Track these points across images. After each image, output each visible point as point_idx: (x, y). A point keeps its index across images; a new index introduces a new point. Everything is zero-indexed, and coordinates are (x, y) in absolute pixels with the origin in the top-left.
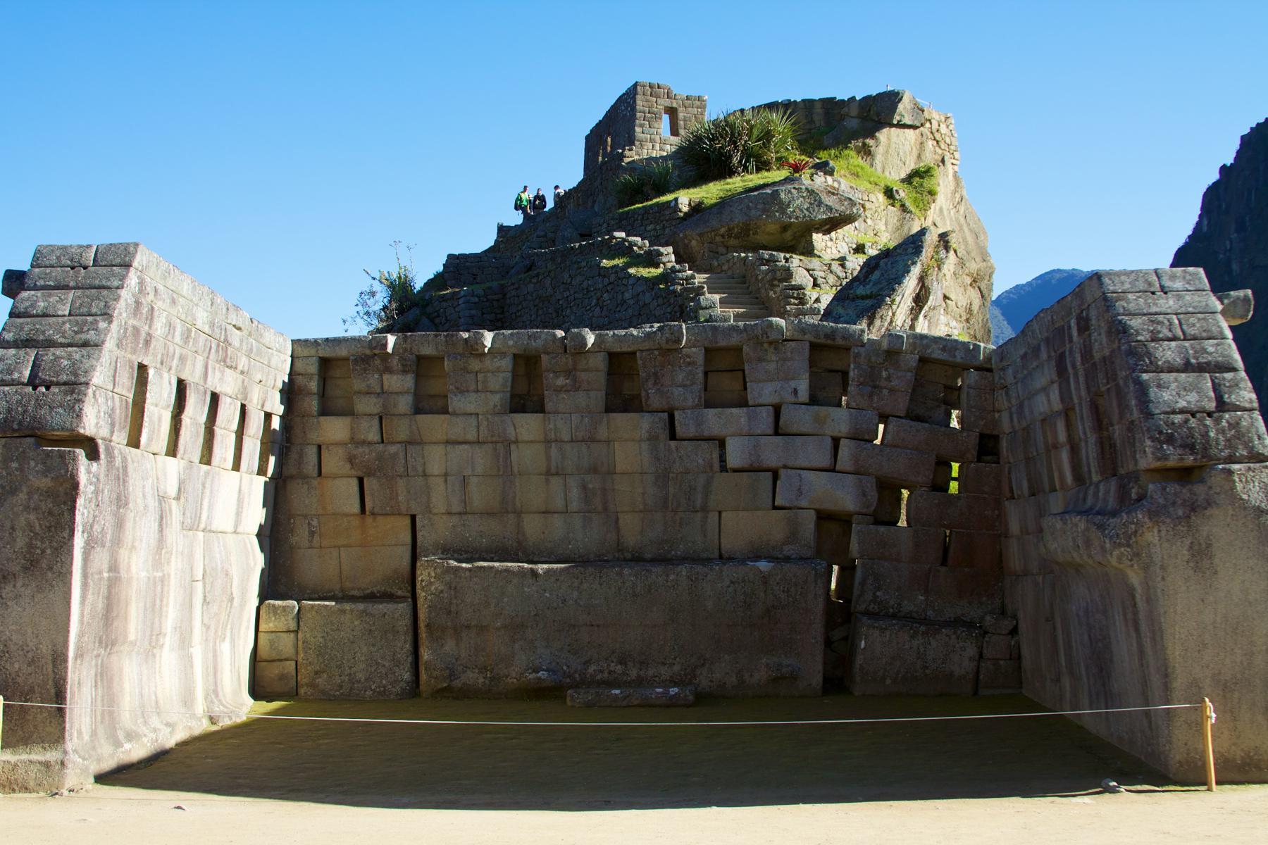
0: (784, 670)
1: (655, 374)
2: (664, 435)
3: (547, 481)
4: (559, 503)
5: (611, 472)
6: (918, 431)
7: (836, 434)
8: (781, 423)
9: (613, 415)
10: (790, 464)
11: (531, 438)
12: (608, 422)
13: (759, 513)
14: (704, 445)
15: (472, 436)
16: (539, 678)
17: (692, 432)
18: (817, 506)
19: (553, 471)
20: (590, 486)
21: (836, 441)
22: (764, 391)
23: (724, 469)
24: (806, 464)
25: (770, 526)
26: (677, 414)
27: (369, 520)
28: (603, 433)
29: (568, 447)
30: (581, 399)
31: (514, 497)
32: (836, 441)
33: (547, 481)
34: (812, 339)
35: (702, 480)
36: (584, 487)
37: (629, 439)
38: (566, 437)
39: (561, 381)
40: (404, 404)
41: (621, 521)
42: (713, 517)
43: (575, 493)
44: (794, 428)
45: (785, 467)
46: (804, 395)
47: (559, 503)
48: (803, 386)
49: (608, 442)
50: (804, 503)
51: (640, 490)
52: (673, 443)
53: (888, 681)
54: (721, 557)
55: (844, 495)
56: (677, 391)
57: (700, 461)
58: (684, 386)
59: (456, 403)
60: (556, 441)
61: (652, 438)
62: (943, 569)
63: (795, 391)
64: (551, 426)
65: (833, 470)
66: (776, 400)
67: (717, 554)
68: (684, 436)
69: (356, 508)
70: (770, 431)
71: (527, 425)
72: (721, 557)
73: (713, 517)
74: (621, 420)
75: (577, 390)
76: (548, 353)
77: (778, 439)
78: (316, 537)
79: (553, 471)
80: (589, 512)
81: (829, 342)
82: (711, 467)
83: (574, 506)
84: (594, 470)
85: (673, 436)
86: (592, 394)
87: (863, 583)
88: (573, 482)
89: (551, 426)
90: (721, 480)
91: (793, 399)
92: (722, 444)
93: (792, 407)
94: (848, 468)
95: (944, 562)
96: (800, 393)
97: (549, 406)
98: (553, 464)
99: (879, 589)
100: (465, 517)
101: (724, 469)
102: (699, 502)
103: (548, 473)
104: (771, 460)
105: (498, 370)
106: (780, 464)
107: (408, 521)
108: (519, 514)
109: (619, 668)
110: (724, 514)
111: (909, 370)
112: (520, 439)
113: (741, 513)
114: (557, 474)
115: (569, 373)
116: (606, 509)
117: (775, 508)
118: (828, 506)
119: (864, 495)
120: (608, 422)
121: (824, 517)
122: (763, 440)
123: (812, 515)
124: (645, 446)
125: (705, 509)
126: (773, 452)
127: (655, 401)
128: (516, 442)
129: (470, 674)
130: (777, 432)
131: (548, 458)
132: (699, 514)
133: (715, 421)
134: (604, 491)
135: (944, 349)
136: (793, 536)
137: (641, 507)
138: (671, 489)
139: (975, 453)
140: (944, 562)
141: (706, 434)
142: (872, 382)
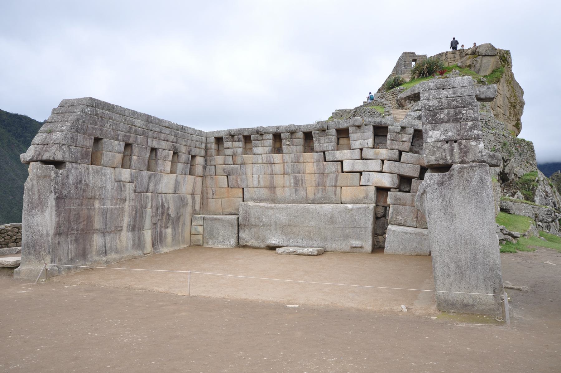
4: (288, 184)
7: (382, 159)
10: (365, 170)
11: (278, 162)
15: (260, 162)
17: (331, 159)
21: (383, 161)
22: (356, 144)
23: (343, 172)
27: (230, 189)
32: (383, 161)
40: (240, 151)
42: (339, 189)
43: (292, 181)
47: (288, 184)
48: (370, 142)
50: (370, 184)
52: (325, 163)
56: (325, 145)
63: (368, 144)
65: (382, 172)
69: (226, 186)
71: (277, 157)
73: (339, 189)
77: (361, 161)
78: (215, 195)
83: (292, 185)
91: (367, 146)
101: (343, 172)
103: (284, 174)
107: (241, 190)
111: (410, 134)
118: (380, 185)
125: (335, 186)
126: (359, 165)
130: (362, 159)
133: (339, 155)
136: (367, 196)
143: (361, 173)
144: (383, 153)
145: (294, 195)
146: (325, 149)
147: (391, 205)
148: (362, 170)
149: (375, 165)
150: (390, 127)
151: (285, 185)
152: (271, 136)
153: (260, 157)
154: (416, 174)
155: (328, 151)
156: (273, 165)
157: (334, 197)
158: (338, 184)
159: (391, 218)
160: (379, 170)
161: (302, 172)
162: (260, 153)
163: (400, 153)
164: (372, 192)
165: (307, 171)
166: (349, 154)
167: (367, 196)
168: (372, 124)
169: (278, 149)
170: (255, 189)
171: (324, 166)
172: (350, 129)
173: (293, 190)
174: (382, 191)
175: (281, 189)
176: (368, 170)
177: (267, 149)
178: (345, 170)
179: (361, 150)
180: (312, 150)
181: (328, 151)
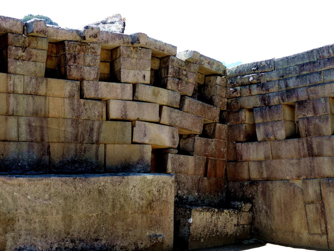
1: (75, 56)
2: (77, 96)
3: (6, 119)
4: (13, 134)
5: (46, 117)
6: (198, 104)
9: (50, 79)
10: (141, 118)
12: (47, 83)
13: (125, 146)
17: (92, 95)
18: (152, 143)
19: (10, 112)
20: (34, 124)
21: (161, 107)
22: (128, 75)
24: (148, 119)
28: (42, 90)
29: (21, 98)
30: (31, 66)
32: (161, 107)
33: (6, 119)
35: (96, 124)
36: (30, 125)
38: (20, 90)
39: (20, 53)
42: (102, 147)
43: (24, 128)
46: (148, 80)
49: (45, 96)
50: (147, 141)
52: (82, 101)
53: (202, 240)
56: (87, 69)
57: (96, 113)
60: (14, 92)
61: (71, 97)
62: (205, 178)
63: (144, 77)
64: (11, 82)
68: (88, 97)
70: (131, 99)
74: (55, 83)
76: (13, 33)
77: (135, 103)
82: (102, 117)
84: (36, 114)
85: (82, 96)
86: (38, 64)
88: (23, 121)
89: (11, 82)
90: (107, 126)
91: (143, 81)
92: (107, 103)
93: (143, 85)
95: (205, 175)
96: (146, 78)
97: (11, 68)
98: (11, 108)
99: (179, 189)
101: (108, 119)
102: (95, 138)
104: (132, 115)
106: (136, 118)
110: (108, 146)
113: (116, 146)
114: (13, 115)
116: (42, 140)
117: (133, 143)
120: (47, 83)
122: (128, 103)
124: (67, 101)
125: (98, 142)
126: (133, 111)
127: (74, 73)
131: (8, 104)
132: (95, 146)
133: (106, 89)
134: (42, 128)
135: (209, 63)
137: (63, 139)
138: (80, 129)
140: (205, 175)
142: (178, 76)
144: (164, 96)
149: (151, 113)
150: (172, 58)
151: (8, 138)
158: (101, 139)
160: (157, 119)
165: (52, 113)
166: (119, 91)
168: (152, 47)
171: (79, 105)
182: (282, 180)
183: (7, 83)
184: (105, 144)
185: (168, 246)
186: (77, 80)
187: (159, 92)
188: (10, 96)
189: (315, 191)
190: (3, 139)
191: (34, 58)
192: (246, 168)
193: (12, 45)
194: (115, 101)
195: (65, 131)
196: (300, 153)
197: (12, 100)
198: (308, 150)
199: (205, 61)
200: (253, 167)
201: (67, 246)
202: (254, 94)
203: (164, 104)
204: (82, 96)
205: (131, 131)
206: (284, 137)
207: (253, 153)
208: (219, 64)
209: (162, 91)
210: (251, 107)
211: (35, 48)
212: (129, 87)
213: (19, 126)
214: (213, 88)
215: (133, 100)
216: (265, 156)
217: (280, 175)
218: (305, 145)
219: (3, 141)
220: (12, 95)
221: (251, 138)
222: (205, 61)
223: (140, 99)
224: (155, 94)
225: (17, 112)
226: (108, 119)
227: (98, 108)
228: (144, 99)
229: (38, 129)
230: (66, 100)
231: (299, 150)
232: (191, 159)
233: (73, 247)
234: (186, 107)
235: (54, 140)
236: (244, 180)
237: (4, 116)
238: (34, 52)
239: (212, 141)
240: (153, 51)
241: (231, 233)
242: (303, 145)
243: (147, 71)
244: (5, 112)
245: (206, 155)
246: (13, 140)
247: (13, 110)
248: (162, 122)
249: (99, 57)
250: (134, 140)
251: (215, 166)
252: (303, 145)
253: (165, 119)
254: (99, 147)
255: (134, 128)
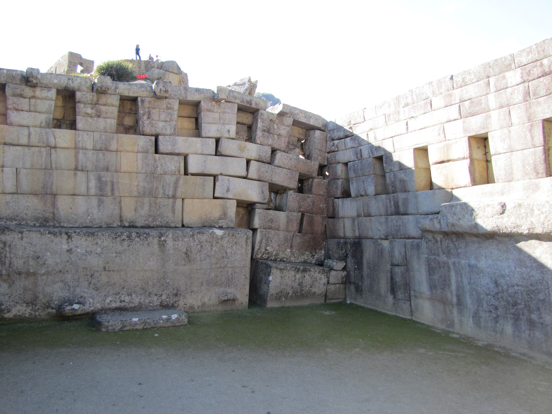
0: (229, 296)
3: (75, 174)
4: (82, 189)
7: (249, 158)
8: (219, 149)
10: (224, 173)
14: (176, 158)
15: (24, 141)
16: (74, 309)
17: (169, 149)
25: (213, 210)
26: (160, 138)
28: (114, 146)
31: (52, 185)
32: (248, 162)
33: (75, 174)
34: (239, 102)
35: (174, 178)
37: (131, 152)
41: (122, 202)
42: (179, 202)
43: (93, 183)
44: (227, 152)
45: (221, 174)
46: (233, 134)
47: (82, 189)
50: (230, 196)
51: (136, 183)
52: (157, 155)
54: (183, 226)
55: (253, 192)
56: (161, 124)
58: (165, 121)
59: (13, 116)
63: (229, 131)
66: (217, 135)
67: (180, 225)
70: (214, 153)
71: (64, 136)
72: (183, 226)
73: (179, 202)
75: (99, 116)
77: (217, 158)
79: (80, 168)
80: (102, 196)
81: (248, 105)
82: (179, 172)
83: (93, 191)
86: (108, 121)
87: (261, 242)
88: (92, 177)
89: (80, 139)
91: (227, 136)
94: (254, 177)
95: (300, 231)
100: (16, 196)
101: (186, 173)
102: (171, 193)
103: (76, 169)
105: (46, 99)
108: (55, 195)
109: (127, 299)
110: (185, 200)
112: (58, 146)
113: (196, 200)
114: (82, 170)
115: (95, 104)
117: (214, 198)
119: (263, 192)
121: (241, 204)
123: (234, 203)
125: (174, 197)
126: (214, 165)
128: (55, 147)
129: (19, 307)
130: (217, 153)
136: (224, 215)
139: (317, 173)
141: (177, 151)
143: (215, 177)
144: (252, 150)
145: (95, 211)
146: (159, 131)
147: (259, 230)
148: (218, 173)
150: (261, 111)
151: (77, 192)
152: (53, 94)
153: (26, 131)
154: (294, 184)
155: (164, 135)
156: (53, 151)
157: (170, 215)
158: (179, 194)
159: (259, 249)
160: (244, 173)
161: (113, 169)
162: (24, 122)
163: (274, 151)
164: (232, 209)
165: (124, 168)
166: (199, 145)
167: (224, 215)
169: (67, 120)
170: (9, 197)
171: (155, 161)
172: (202, 103)
173: (94, 201)
174: (247, 208)
175: (68, 199)
176: (228, 173)
177: (42, 118)
178: (191, 170)
179: (218, 141)
180: (134, 129)
181: (164, 135)
182: (372, 239)
183: (75, 140)
184: (183, 199)
185: (242, 303)
186: (152, 135)
187: (245, 147)
188: (79, 152)
189: (400, 253)
190: (72, 193)
191: (103, 115)
192: (342, 225)
193: (79, 102)
194: (195, 156)
195: (137, 185)
196: (387, 211)
197: (81, 156)
198: (395, 207)
199: (301, 115)
200: (348, 223)
201: (122, 299)
202: (348, 147)
203: (252, 158)
204: (157, 151)
205: (213, 186)
206: (374, 193)
207: (347, 208)
208: (318, 118)
209: (250, 145)
210: (347, 161)
211: (104, 105)
212: (212, 142)
213: (88, 181)
214: (312, 142)
215: (216, 155)
216: (358, 213)
217: (370, 234)
218: (392, 202)
219: (72, 195)
220: (81, 151)
221: (346, 194)
222: (301, 115)
223: (223, 153)
224: (242, 149)
225: (86, 168)
226: (186, 173)
227: (176, 164)
228: (227, 154)
229: (109, 184)
230: (138, 154)
231: (387, 207)
232: (282, 215)
233: (130, 301)
234: (277, 162)
235: (126, 195)
236: (340, 238)
237: (73, 172)
238: (103, 108)
239: (309, 197)
240: (238, 104)
241: (320, 292)
242: (390, 202)
243: (232, 126)
244: (74, 167)
245: (301, 211)
246: (82, 194)
247: (82, 166)
248: (249, 176)
249: (176, 113)
250: (216, 195)
251: (311, 223)
252: (390, 202)
253: (253, 173)
254: (175, 202)
255: (217, 183)
